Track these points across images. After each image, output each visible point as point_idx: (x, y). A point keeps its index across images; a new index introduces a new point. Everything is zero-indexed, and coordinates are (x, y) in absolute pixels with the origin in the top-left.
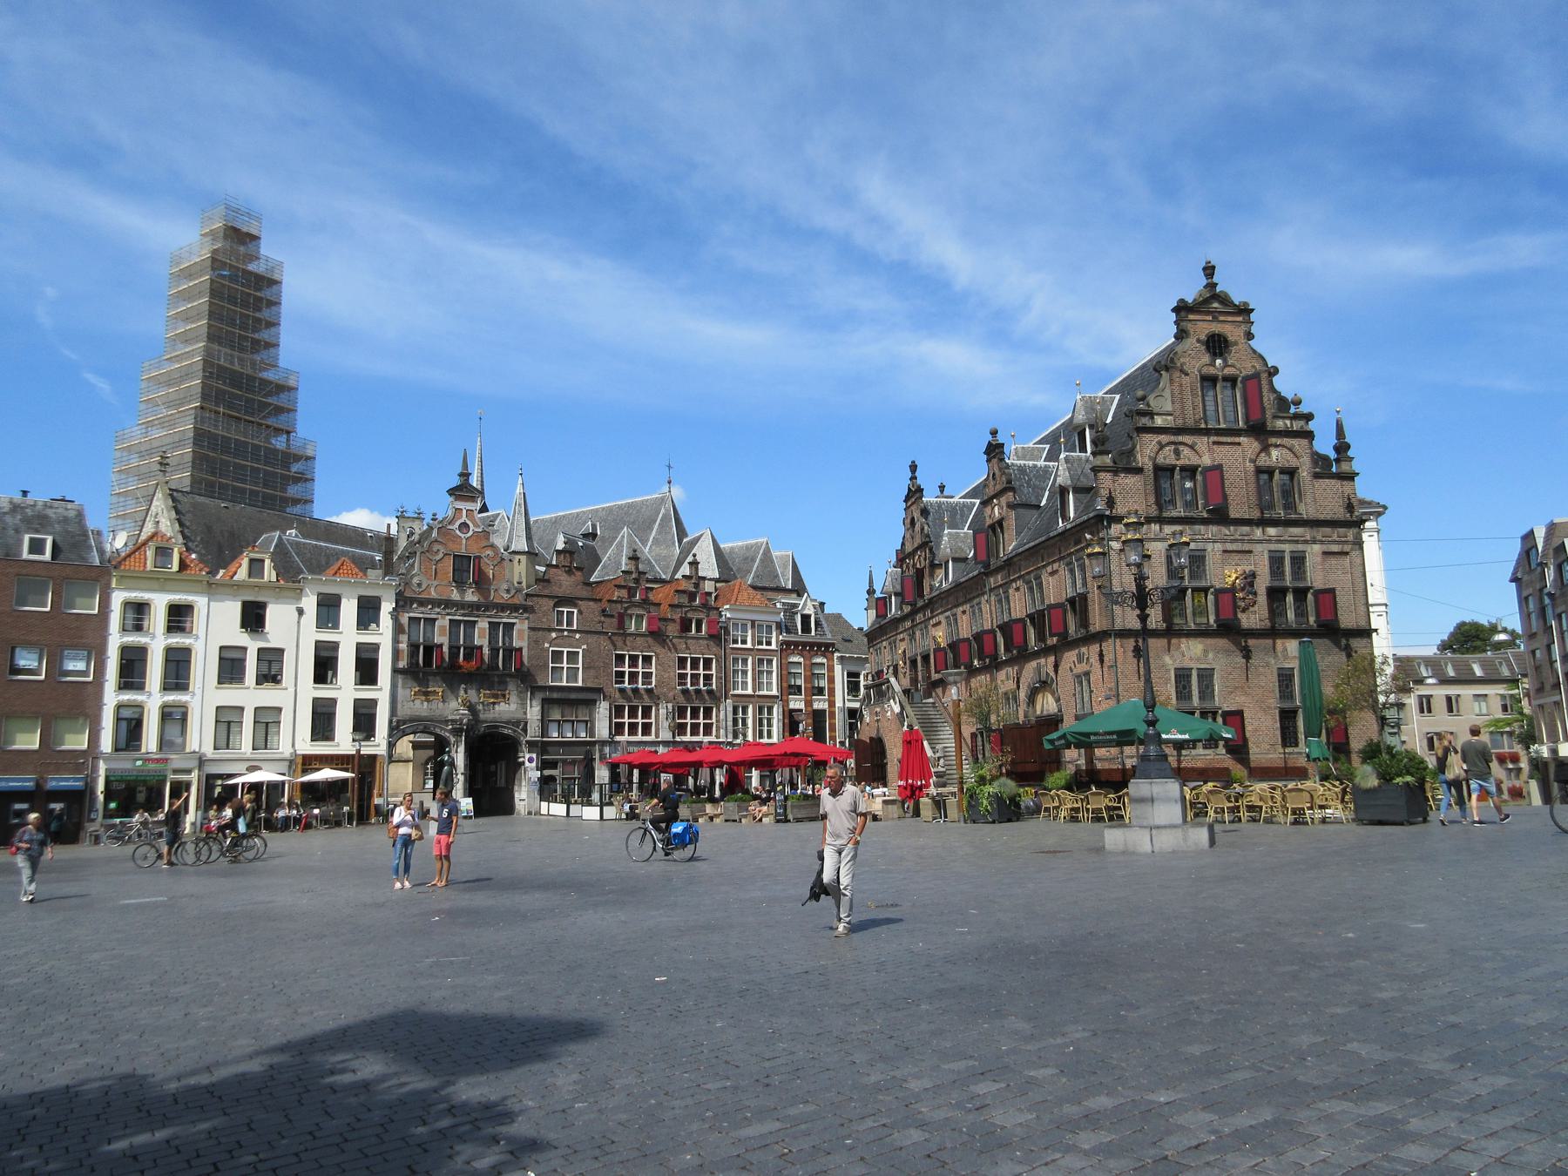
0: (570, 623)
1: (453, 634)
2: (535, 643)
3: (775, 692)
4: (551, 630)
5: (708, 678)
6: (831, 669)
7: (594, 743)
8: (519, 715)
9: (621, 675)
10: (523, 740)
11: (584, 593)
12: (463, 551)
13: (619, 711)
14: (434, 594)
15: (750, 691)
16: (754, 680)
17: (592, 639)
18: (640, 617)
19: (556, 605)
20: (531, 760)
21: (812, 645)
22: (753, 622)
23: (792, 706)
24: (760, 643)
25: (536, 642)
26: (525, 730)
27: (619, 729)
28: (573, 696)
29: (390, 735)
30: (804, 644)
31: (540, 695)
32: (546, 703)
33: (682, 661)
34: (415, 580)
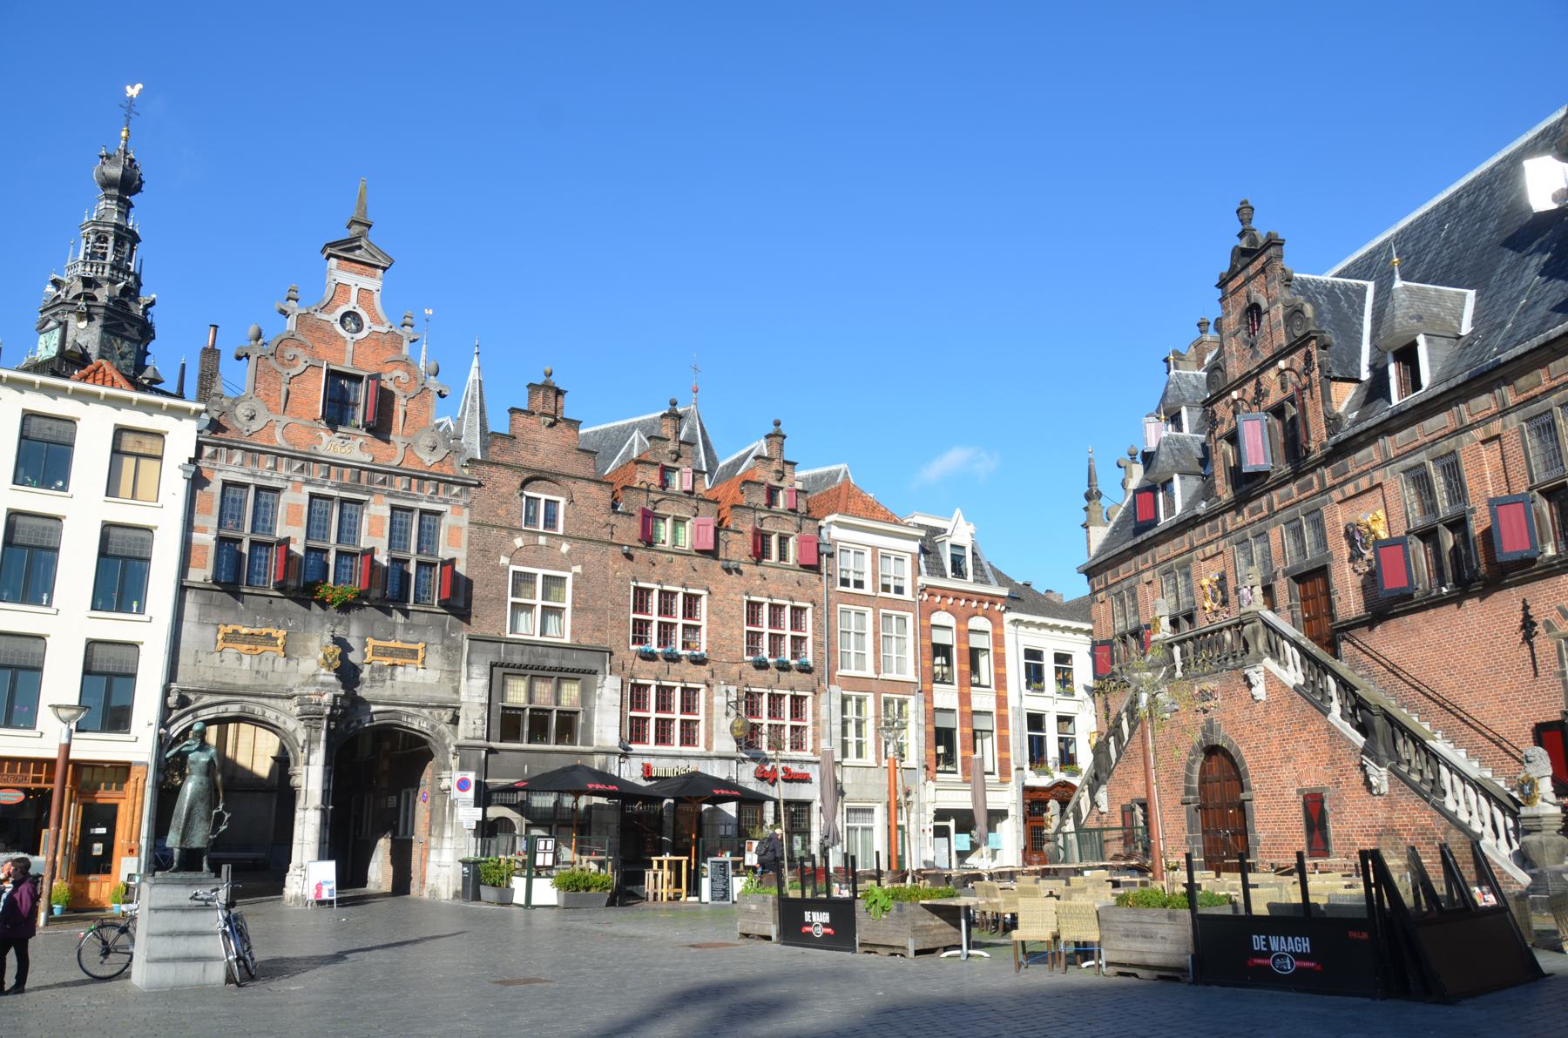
0: (550, 521)
1: (315, 525)
2: (482, 552)
3: (910, 675)
4: (513, 530)
5: (797, 641)
6: (999, 641)
7: (592, 753)
8: (444, 694)
9: (641, 628)
10: (451, 743)
11: (580, 470)
12: (346, 367)
13: (637, 695)
14: (279, 441)
15: (869, 672)
16: (876, 652)
17: (592, 554)
18: (679, 521)
19: (524, 485)
20: (463, 785)
21: (969, 596)
22: (875, 549)
23: (937, 704)
24: (886, 588)
25: (484, 552)
26: (455, 721)
27: (636, 730)
28: (553, 663)
29: (164, 723)
30: (958, 594)
31: (490, 654)
32: (500, 672)
33: (754, 607)
34: (242, 411)
